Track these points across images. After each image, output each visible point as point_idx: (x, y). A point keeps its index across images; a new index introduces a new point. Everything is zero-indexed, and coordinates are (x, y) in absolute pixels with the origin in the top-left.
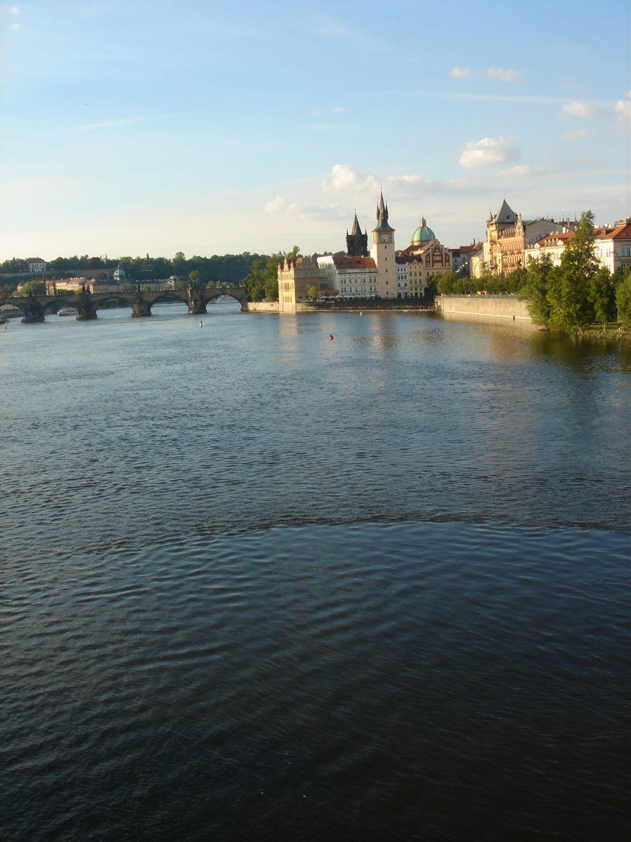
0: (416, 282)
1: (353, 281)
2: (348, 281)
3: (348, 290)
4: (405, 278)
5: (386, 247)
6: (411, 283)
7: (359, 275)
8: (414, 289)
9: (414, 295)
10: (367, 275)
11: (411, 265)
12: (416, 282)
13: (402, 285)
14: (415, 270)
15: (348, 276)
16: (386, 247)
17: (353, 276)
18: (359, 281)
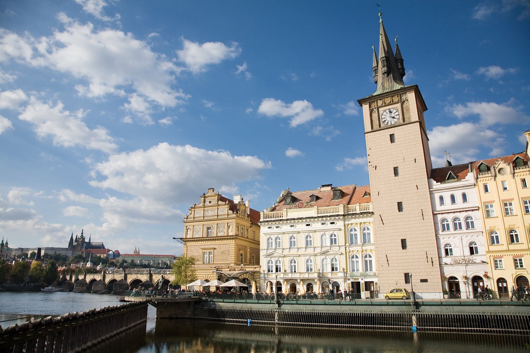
0: (513, 238)
1: (301, 241)
2: (285, 241)
3: (285, 265)
4: (470, 225)
5: (392, 137)
6: (494, 240)
7: (316, 225)
8: (508, 262)
9: (511, 285)
10: (340, 224)
11: (486, 178)
12: (513, 238)
13: (460, 250)
14: (505, 196)
15: (286, 228)
16: (392, 137)
17: (301, 226)
18: (316, 239)
